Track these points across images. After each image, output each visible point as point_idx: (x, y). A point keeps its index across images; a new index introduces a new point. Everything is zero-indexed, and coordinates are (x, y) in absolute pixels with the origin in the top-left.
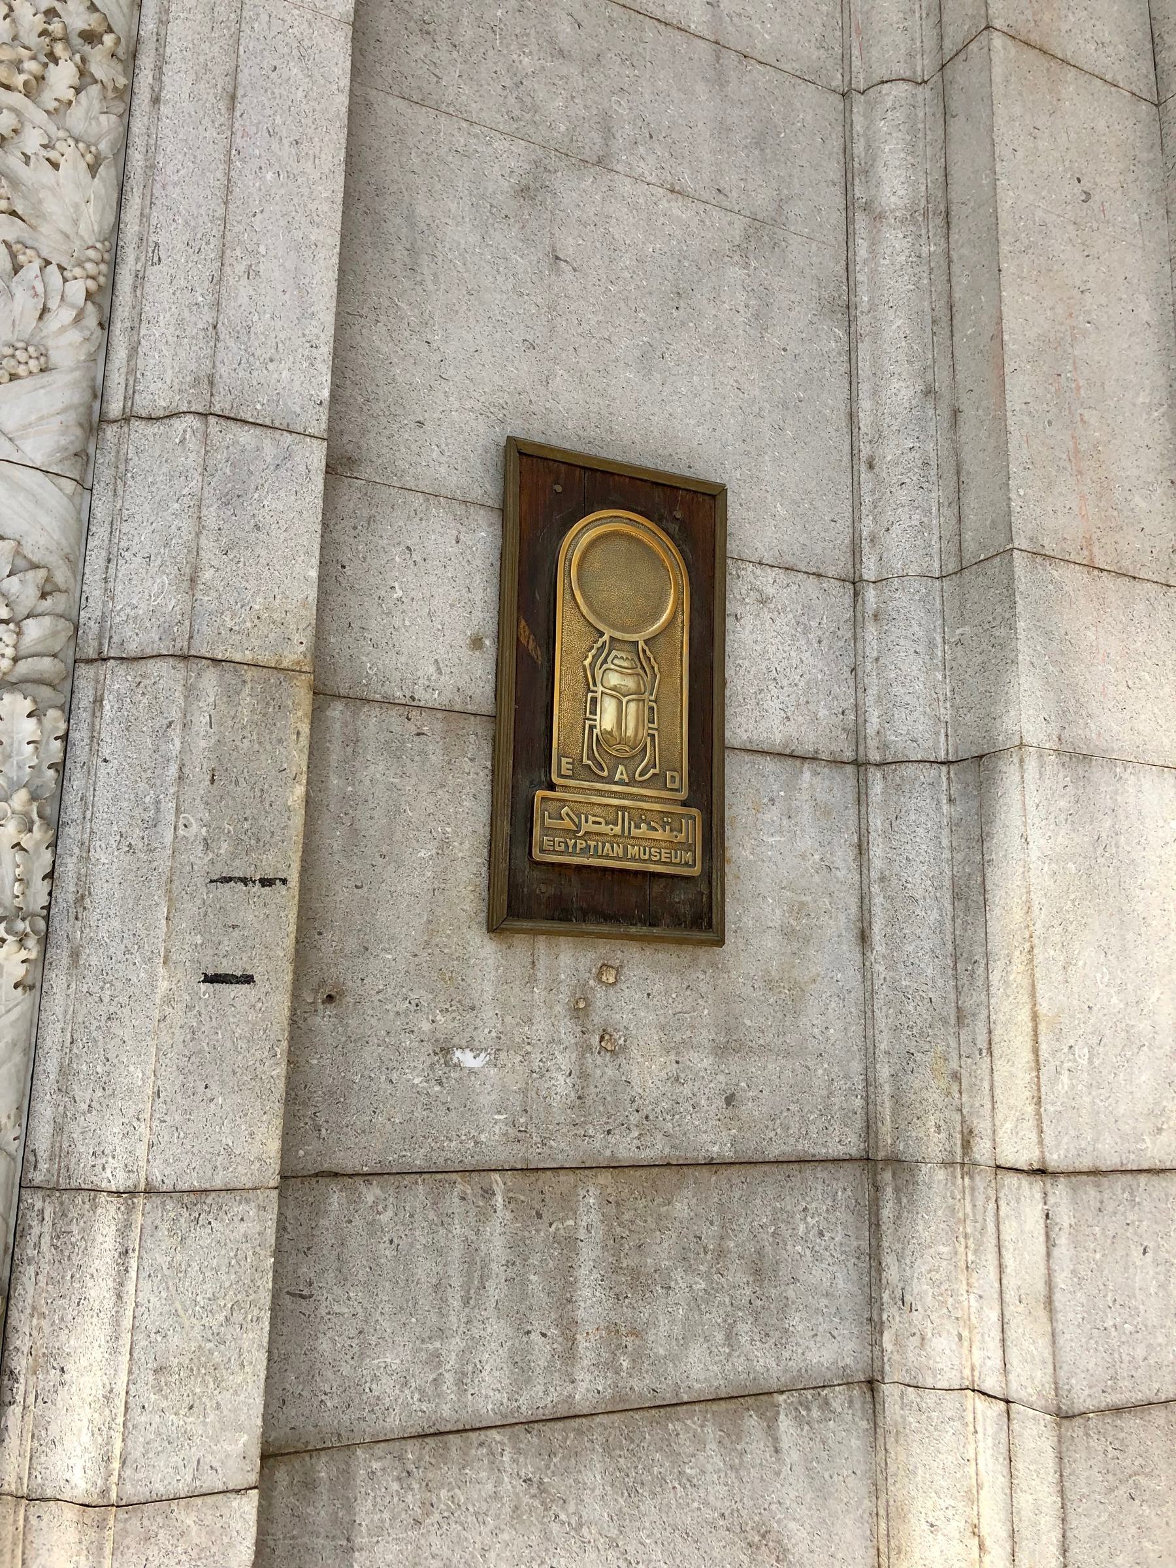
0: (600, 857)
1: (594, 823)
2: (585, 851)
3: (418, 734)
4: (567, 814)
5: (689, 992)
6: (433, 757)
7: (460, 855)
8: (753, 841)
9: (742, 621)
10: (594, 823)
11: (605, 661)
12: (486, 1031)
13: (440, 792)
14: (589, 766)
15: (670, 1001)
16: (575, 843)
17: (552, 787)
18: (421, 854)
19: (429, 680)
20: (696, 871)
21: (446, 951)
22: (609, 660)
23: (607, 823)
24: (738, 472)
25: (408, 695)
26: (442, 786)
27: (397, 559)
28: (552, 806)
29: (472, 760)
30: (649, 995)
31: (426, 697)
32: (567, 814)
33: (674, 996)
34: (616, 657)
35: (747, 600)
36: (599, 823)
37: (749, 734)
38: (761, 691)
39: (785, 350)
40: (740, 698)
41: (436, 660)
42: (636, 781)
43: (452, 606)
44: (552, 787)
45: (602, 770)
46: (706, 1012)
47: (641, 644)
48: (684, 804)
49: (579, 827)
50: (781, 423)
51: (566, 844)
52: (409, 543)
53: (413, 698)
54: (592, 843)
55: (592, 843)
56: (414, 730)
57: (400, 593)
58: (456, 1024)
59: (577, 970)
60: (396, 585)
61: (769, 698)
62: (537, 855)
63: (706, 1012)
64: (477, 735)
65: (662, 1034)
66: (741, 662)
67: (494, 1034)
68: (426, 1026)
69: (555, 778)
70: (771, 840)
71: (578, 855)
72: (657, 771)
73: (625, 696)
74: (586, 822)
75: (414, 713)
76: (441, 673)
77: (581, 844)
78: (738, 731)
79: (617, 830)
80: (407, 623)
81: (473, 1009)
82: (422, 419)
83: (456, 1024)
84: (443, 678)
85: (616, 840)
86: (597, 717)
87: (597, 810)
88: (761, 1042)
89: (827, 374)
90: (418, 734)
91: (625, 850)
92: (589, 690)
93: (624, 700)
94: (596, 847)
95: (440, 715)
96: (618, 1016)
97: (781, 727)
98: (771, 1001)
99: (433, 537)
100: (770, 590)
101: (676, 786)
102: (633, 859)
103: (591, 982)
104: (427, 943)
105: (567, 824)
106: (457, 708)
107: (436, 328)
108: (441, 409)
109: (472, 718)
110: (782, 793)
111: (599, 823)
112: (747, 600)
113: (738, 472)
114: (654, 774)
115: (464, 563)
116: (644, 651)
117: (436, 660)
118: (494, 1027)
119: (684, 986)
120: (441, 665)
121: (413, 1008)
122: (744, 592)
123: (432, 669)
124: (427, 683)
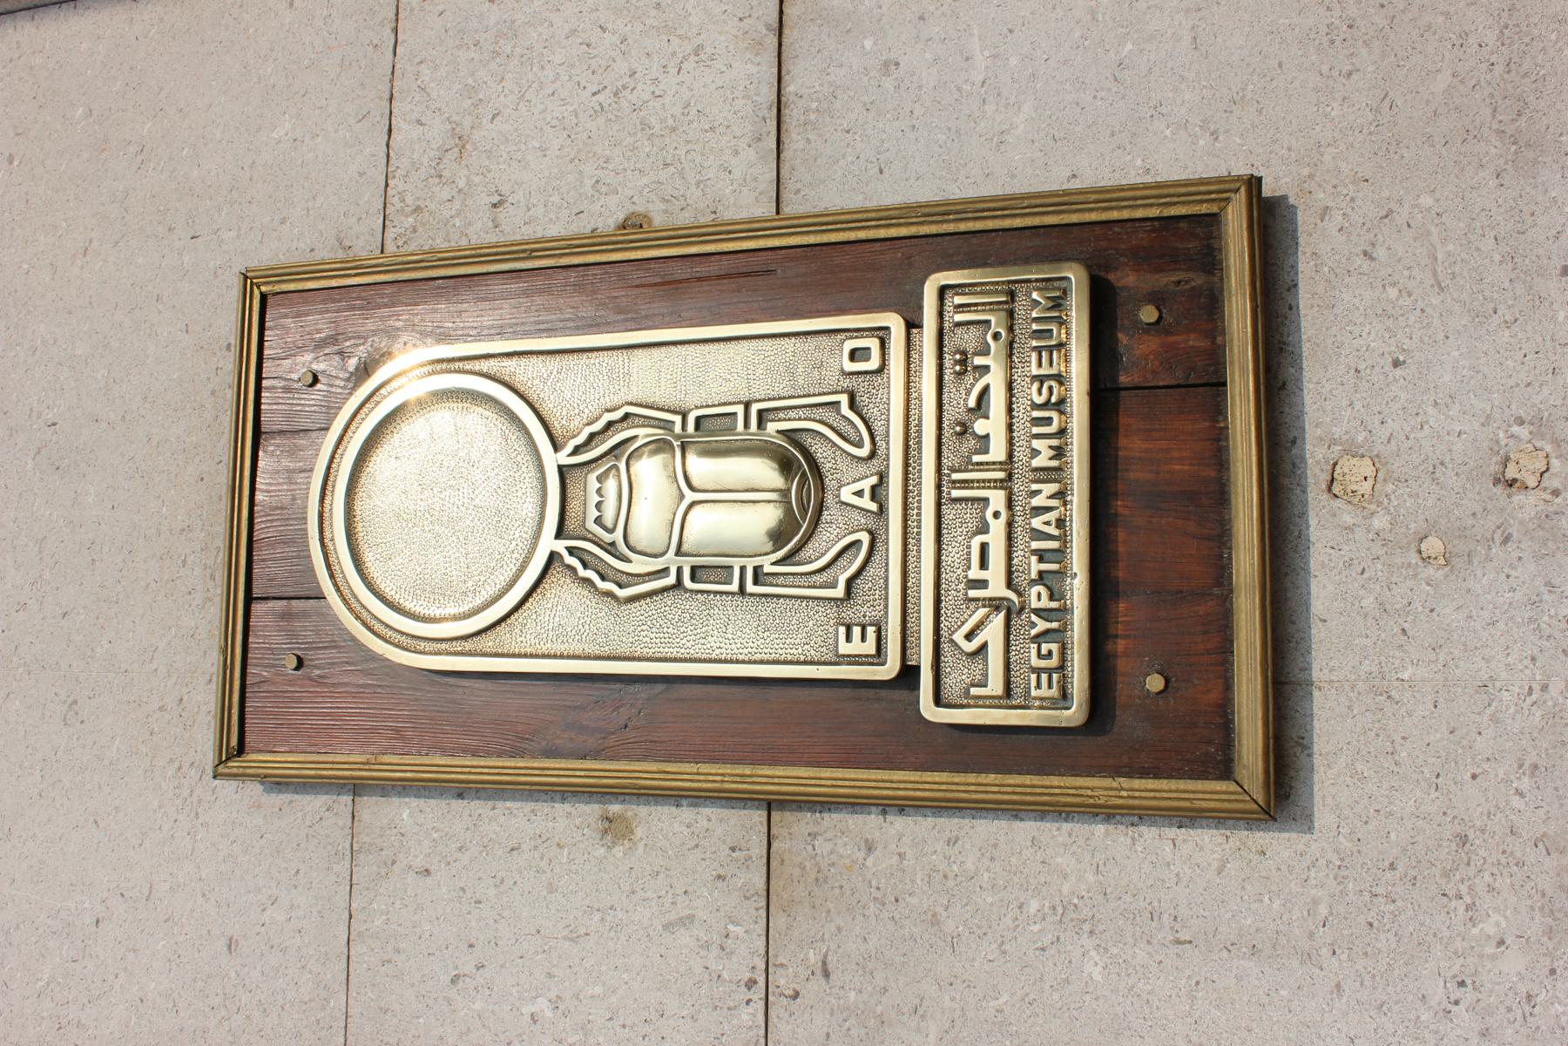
0: (1064, 539)
1: (983, 565)
2: (1052, 582)
3: (826, 974)
4: (969, 636)
5: (1380, 253)
6: (873, 941)
7: (1090, 877)
8: (990, 108)
9: (505, 189)
10: (983, 565)
11: (611, 548)
12: (1516, 802)
13: (950, 926)
14: (850, 582)
15: (1406, 302)
16: (1037, 612)
17: (909, 674)
18: (1097, 977)
19: (707, 946)
20: (1075, 277)
21: (1323, 910)
22: (607, 537)
23: (984, 529)
24: (227, 235)
25: (743, 994)
26: (935, 921)
27: (478, 1006)
28: (955, 680)
29: (870, 848)
30: (1396, 364)
31: (745, 956)
32: (969, 636)
33: (1392, 293)
34: (598, 521)
35: (462, 183)
36: (984, 548)
37: (742, 144)
38: (645, 126)
39: (11, 160)
40: (663, 175)
41: (665, 927)
42: (873, 455)
43: (552, 889)
44: (909, 674)
45: (857, 543)
46: (1427, 201)
47: (563, 458)
48: (913, 325)
49: (995, 604)
50: (132, 149)
51: (1038, 639)
52: (445, 979)
53: (751, 984)
54: (1035, 567)
55: (1035, 567)
56: (819, 982)
57: (542, 1005)
58: (1503, 883)
59: (1349, 564)
60: (527, 1010)
61: (657, 103)
62: (1074, 714)
63: (1427, 201)
64: (813, 835)
65: (1496, 320)
66: (589, 183)
67: (1526, 783)
68: (1513, 963)
69: (889, 669)
70: (980, 61)
71: (1064, 611)
72: (844, 399)
73: (682, 496)
74: (982, 584)
75: (780, 979)
76: (691, 917)
77: (1038, 597)
78: (737, 174)
79: (997, 499)
80: (598, 990)
81: (1463, 840)
82: (224, 941)
83: (1503, 883)
84: (701, 914)
85: (1020, 500)
86: (736, 564)
87: (952, 556)
88: (1491, 38)
89: (39, 60)
90: (826, 974)
91: (1045, 474)
92: (679, 583)
93: (690, 496)
94: (1042, 556)
95: (778, 921)
96: (1458, 446)
97: (719, 64)
98: (1380, 21)
99: (427, 927)
100: (437, 130)
101: (873, 344)
102: (1059, 452)
103: (1380, 522)
104: (1308, 957)
105: (993, 632)
106: (760, 883)
107: (72, 905)
108: (201, 900)
109: (775, 845)
110: (868, 44)
111: (984, 548)
112: (462, 183)
113: (227, 235)
114: (852, 405)
115: (465, 858)
116: (577, 451)
117: (665, 927)
118: (1508, 782)
119: (1366, 265)
120: (673, 916)
121: (1468, 995)
122: (446, 193)
123: (685, 938)
124: (715, 951)
